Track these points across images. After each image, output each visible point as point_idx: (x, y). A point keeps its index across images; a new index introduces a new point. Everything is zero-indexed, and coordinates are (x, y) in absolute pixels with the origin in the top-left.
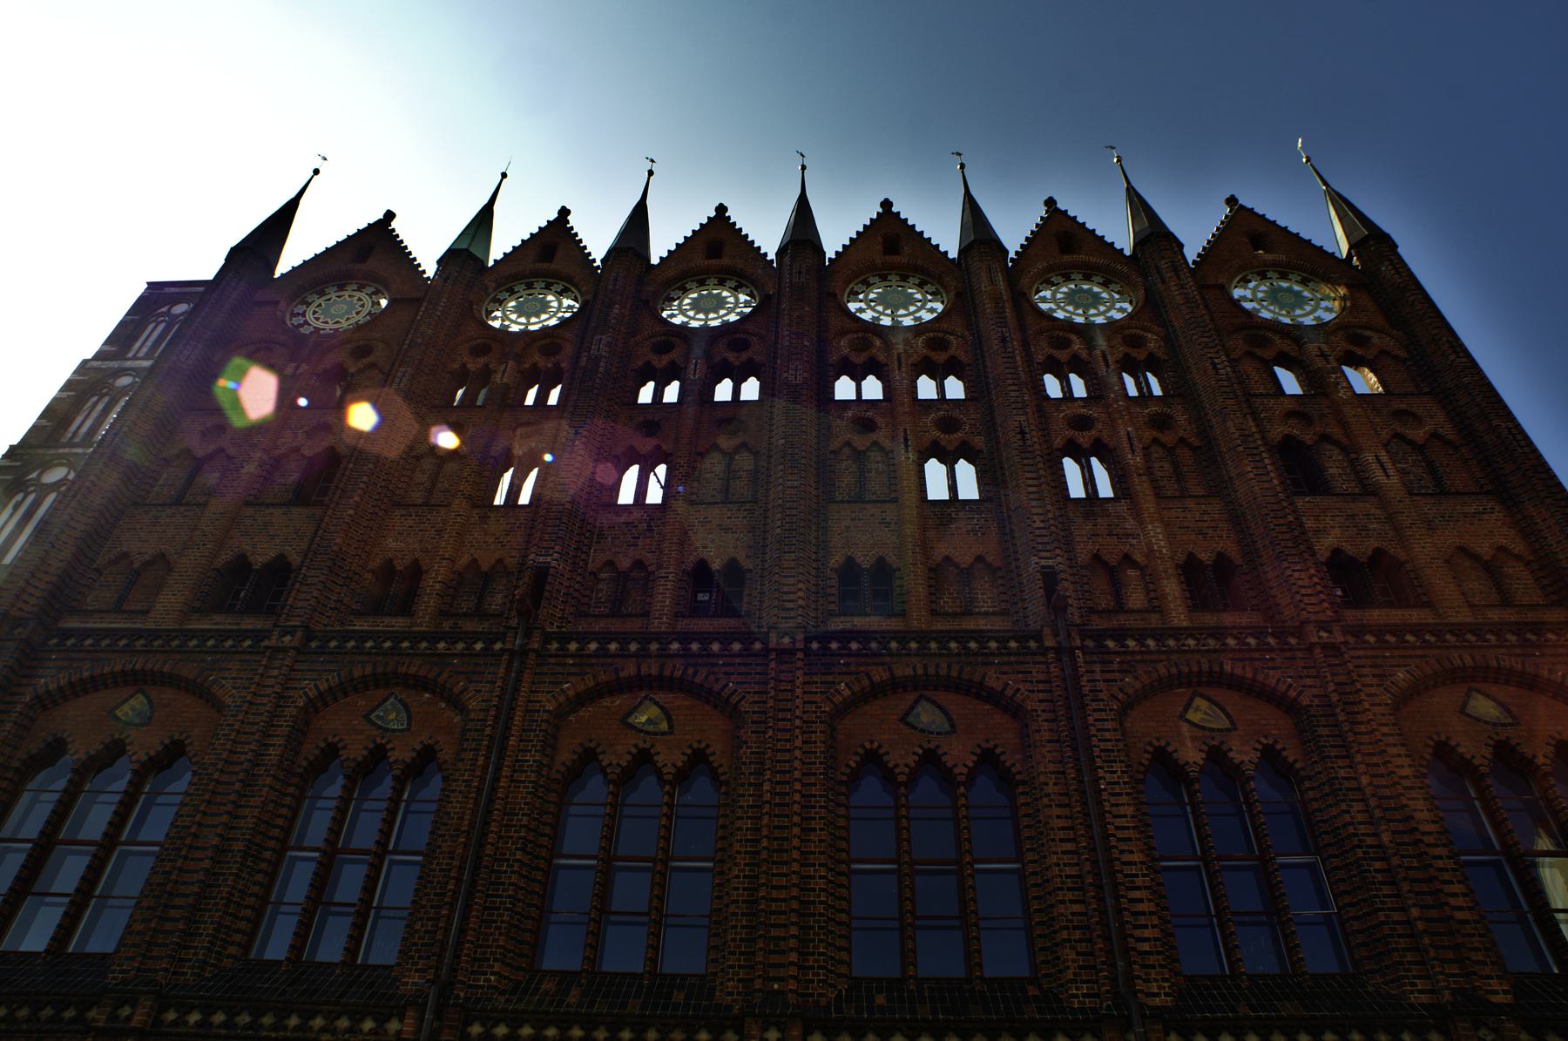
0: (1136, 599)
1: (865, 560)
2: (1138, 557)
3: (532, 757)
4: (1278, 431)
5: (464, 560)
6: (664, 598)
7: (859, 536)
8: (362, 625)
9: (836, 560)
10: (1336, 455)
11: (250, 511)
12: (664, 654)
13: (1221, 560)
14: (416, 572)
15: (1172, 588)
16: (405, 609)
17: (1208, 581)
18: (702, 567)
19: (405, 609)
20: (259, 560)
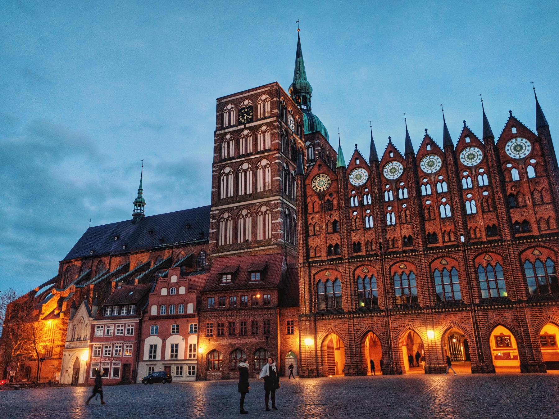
0: (478, 235)
1: (431, 233)
2: (479, 227)
3: (388, 276)
4: (509, 192)
5: (366, 240)
6: (400, 244)
7: (430, 228)
8: (355, 254)
9: (427, 233)
10: (521, 196)
11: (327, 235)
12: (403, 257)
13: (494, 225)
14: (359, 243)
15: (484, 233)
16: (360, 250)
17: (492, 230)
18: (405, 236)
19: (360, 250)
20: (334, 245)
